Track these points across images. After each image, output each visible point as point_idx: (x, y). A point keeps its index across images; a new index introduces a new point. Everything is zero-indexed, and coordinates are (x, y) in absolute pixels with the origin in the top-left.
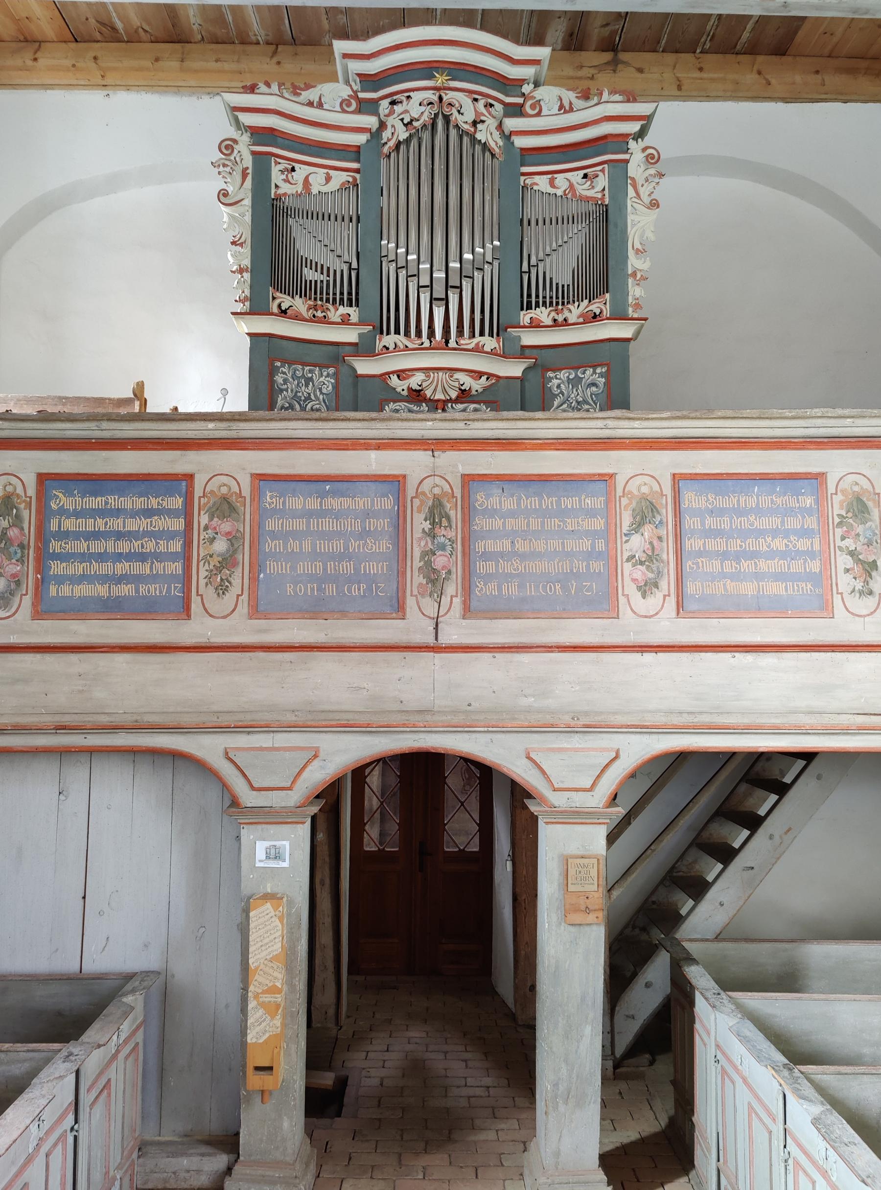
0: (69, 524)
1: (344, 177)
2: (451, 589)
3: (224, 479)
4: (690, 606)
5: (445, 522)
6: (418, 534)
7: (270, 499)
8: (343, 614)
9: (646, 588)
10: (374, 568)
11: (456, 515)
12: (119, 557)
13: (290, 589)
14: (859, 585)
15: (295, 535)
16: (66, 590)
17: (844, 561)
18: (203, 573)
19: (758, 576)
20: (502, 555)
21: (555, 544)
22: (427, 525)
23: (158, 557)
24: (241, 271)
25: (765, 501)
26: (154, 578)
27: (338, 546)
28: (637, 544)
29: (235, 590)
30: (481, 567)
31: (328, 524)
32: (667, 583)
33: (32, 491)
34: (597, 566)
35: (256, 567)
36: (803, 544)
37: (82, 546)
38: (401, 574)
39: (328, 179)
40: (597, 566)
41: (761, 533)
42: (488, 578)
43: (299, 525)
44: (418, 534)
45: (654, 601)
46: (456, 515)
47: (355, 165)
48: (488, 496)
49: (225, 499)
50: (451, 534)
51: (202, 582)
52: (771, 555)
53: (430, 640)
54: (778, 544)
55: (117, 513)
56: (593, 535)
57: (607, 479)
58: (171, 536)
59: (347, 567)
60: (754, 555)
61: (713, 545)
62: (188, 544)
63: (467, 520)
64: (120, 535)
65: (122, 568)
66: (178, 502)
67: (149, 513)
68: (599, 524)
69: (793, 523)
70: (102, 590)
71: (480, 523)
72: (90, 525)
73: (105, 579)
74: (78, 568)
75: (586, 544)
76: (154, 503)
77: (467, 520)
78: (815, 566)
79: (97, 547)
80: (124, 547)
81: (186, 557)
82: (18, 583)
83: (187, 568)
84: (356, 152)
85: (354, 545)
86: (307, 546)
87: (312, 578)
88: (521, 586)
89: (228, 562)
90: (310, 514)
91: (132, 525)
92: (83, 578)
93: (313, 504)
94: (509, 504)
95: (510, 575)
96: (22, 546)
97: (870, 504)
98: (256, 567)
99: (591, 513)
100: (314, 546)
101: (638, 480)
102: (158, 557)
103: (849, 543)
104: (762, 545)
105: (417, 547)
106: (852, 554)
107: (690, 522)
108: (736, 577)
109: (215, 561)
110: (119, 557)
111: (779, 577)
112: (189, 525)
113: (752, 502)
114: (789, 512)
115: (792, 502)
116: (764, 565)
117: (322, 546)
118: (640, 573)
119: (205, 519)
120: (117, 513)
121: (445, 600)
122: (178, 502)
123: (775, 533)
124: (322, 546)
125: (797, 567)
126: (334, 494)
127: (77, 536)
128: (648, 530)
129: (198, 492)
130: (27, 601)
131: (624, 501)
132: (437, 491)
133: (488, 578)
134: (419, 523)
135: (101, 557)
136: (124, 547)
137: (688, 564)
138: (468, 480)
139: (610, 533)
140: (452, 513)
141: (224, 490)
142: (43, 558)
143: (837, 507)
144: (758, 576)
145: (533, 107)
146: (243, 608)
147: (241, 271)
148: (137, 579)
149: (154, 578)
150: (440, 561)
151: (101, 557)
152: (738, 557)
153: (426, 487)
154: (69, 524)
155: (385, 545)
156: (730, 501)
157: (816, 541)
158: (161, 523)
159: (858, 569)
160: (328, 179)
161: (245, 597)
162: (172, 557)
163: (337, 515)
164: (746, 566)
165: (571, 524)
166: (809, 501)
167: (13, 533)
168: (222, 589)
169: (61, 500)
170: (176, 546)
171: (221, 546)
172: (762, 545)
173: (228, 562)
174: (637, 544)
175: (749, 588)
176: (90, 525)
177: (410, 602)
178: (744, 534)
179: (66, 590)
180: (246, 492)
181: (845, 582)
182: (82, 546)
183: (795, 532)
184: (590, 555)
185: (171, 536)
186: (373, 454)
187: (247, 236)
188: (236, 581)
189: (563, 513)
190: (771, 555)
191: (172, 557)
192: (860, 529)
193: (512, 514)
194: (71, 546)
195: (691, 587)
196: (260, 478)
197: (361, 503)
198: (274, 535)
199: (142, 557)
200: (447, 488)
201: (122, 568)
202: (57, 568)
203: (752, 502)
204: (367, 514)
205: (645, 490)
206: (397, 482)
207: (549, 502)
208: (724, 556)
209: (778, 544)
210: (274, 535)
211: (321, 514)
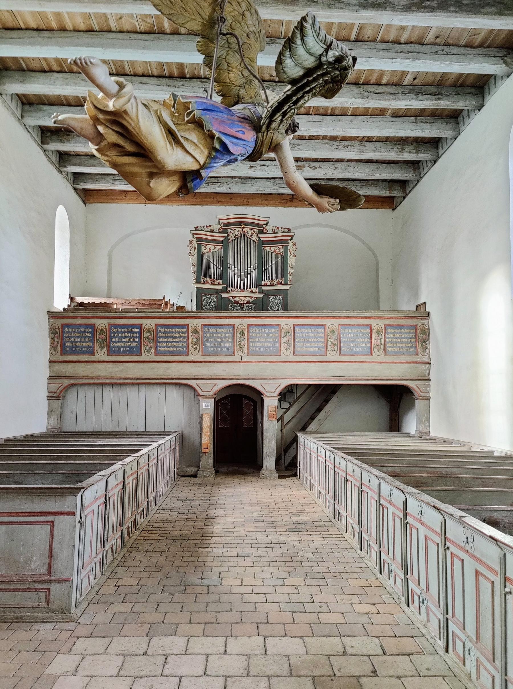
0: (162, 335)
1: (219, 247)
2: (245, 349)
3: (195, 325)
4: (296, 353)
5: (243, 335)
6: (238, 337)
7: (205, 329)
8: (221, 355)
9: (287, 349)
10: (228, 344)
11: (246, 333)
12: (173, 342)
13: (210, 349)
14: (332, 349)
15: (211, 337)
16: (161, 349)
17: (329, 343)
18: (191, 346)
19: (311, 347)
20: (256, 342)
21: (267, 340)
22: (240, 335)
23: (181, 342)
24: (194, 272)
25: (313, 330)
26: (180, 347)
27: (220, 340)
28: (285, 340)
29: (198, 349)
30: (251, 344)
31: (218, 335)
32: (291, 348)
33: (154, 328)
34: (276, 344)
35: (203, 344)
36: (321, 340)
37: (165, 340)
38: (234, 346)
39: (215, 248)
40: (276, 344)
41: (312, 337)
42: (253, 347)
43: (212, 335)
44: (238, 337)
45: (288, 352)
46: (246, 333)
47: (222, 245)
48: (253, 329)
49: (196, 329)
50: (245, 337)
51: (191, 347)
52: (314, 342)
53: (240, 360)
54: (316, 340)
55: (172, 332)
56: (276, 337)
57: (278, 326)
58: (184, 337)
59: (222, 344)
60: (310, 342)
61: (301, 340)
62: (188, 340)
63: (248, 334)
64: (173, 337)
65: (173, 344)
66: (185, 330)
67: (179, 332)
68: (277, 335)
69: (319, 335)
70: (169, 349)
71: (251, 335)
72: (166, 335)
73: (169, 347)
74: (164, 345)
75: (274, 339)
76: (180, 330)
77: (248, 334)
78: (323, 345)
79: (168, 340)
80: (174, 340)
81: (187, 342)
82: (151, 348)
83: (188, 344)
84: (222, 242)
85: (224, 339)
86: (213, 340)
87: (215, 347)
88: (260, 349)
89: (196, 343)
90: (214, 333)
91: (176, 335)
92: (165, 347)
93: (215, 331)
94: (258, 331)
95: (258, 346)
96: (152, 340)
97: (335, 331)
98: (203, 344)
99: (275, 333)
100: (215, 340)
101: (286, 326)
102: (181, 342)
103: (331, 340)
104: (312, 340)
105: (238, 339)
106: (331, 342)
107: (296, 335)
108: (306, 347)
109: (194, 343)
110: (173, 342)
111: (316, 347)
112: (188, 335)
113: (310, 331)
114: (318, 333)
115: (319, 331)
116: (312, 344)
117: (217, 340)
118: (286, 346)
119: (191, 334)
120: (172, 332)
121: (244, 352)
122: (185, 330)
123: (315, 337)
124: (217, 340)
125: (319, 345)
126: (220, 328)
127: (164, 337)
128: (287, 336)
129: (190, 328)
130: (153, 351)
131: (283, 330)
132: (242, 328)
133: (253, 347)
134: (238, 335)
135: (169, 342)
136: (174, 340)
137: (296, 344)
138: (249, 325)
139: (280, 337)
140: (245, 333)
141: (196, 327)
142: (157, 342)
143: (328, 331)
144: (311, 347)
145: (265, 230)
146: (200, 353)
147: (194, 272)
148: (177, 347)
149: (180, 347)
150: (242, 343)
151: (169, 342)
152: (307, 342)
153: (239, 327)
154: (162, 335)
155: (231, 340)
156: (306, 330)
157: (324, 339)
158: (181, 335)
159: (332, 345)
160: (215, 248)
161: (200, 351)
162: (185, 342)
163: (220, 333)
164: (308, 344)
165: (271, 335)
166: (322, 330)
167: (150, 337)
168: (195, 349)
169: (160, 329)
170: (185, 340)
171: (195, 340)
172: (312, 340)
173: (196, 343)
174: (285, 340)
175: (309, 349)
176: (166, 335)
177: (236, 352)
178: (308, 337)
179: (161, 349)
180: (200, 328)
181: (329, 348)
182: (165, 340)
183: (319, 337)
184: (275, 342)
185: (184, 337)
186: (228, 320)
187: (196, 263)
188: (198, 348)
189: (270, 333)
190: (314, 342)
191: (185, 342)
192: (333, 337)
193: (258, 333)
194: (162, 340)
195: (296, 349)
196: (204, 325)
197: (225, 330)
198: (206, 337)
199: (178, 342)
200: (244, 327)
201: (173, 344)
202: (159, 344)
203: (310, 331)
204: (227, 333)
205: (287, 328)
206: (233, 326)
207: (266, 330)
208: (304, 342)
209: (316, 340)
210: (206, 337)
211: (217, 333)
